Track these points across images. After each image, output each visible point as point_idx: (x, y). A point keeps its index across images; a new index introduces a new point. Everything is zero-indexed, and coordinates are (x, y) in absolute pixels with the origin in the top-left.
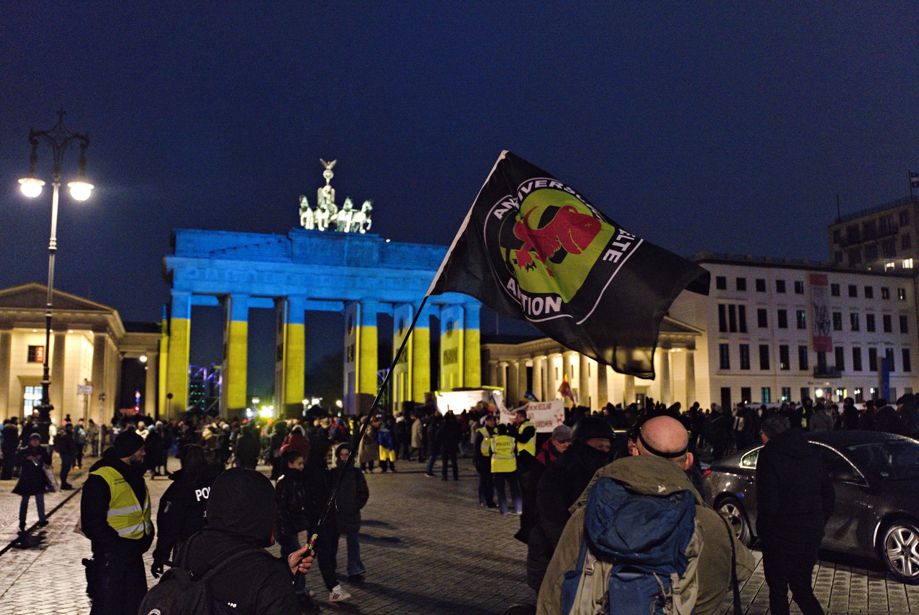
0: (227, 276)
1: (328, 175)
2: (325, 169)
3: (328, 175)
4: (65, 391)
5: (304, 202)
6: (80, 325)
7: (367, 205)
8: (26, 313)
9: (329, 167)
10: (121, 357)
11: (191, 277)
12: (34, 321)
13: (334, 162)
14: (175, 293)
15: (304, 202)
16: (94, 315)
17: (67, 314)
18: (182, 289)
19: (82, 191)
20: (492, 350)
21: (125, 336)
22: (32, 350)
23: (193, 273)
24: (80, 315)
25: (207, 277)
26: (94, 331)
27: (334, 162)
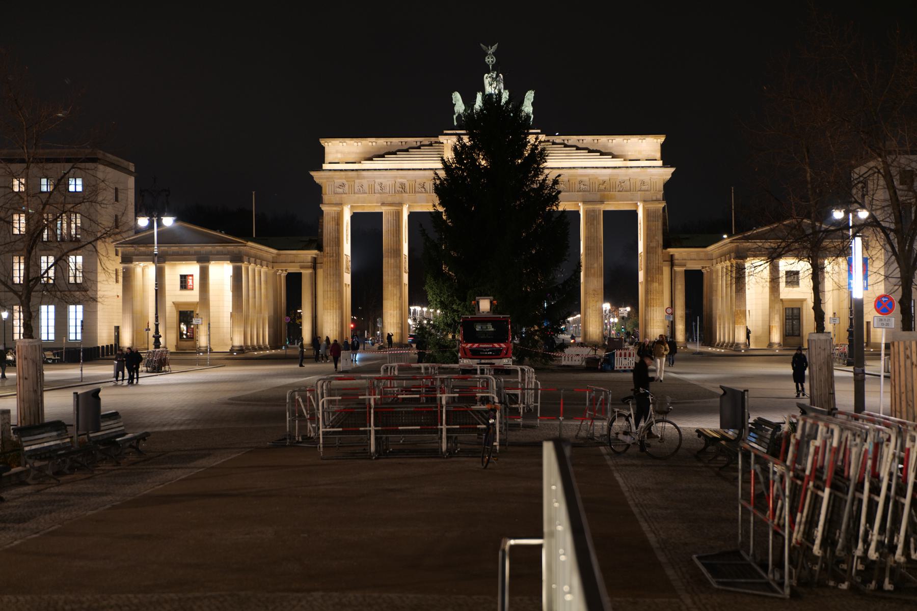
0: (378, 187)
1: (490, 60)
2: (486, 54)
3: (490, 60)
4: (211, 314)
5: (457, 97)
6: (220, 257)
7: (530, 96)
8: (174, 249)
9: (491, 50)
10: (284, 274)
11: (341, 190)
12: (181, 255)
13: (495, 47)
14: (324, 208)
15: (457, 97)
16: (231, 248)
17: (208, 248)
18: (330, 204)
19: (168, 221)
20: (677, 256)
21: (279, 255)
22: (184, 279)
23: (343, 185)
24: (219, 248)
25: (356, 188)
26: (232, 261)
27: (495, 47)
